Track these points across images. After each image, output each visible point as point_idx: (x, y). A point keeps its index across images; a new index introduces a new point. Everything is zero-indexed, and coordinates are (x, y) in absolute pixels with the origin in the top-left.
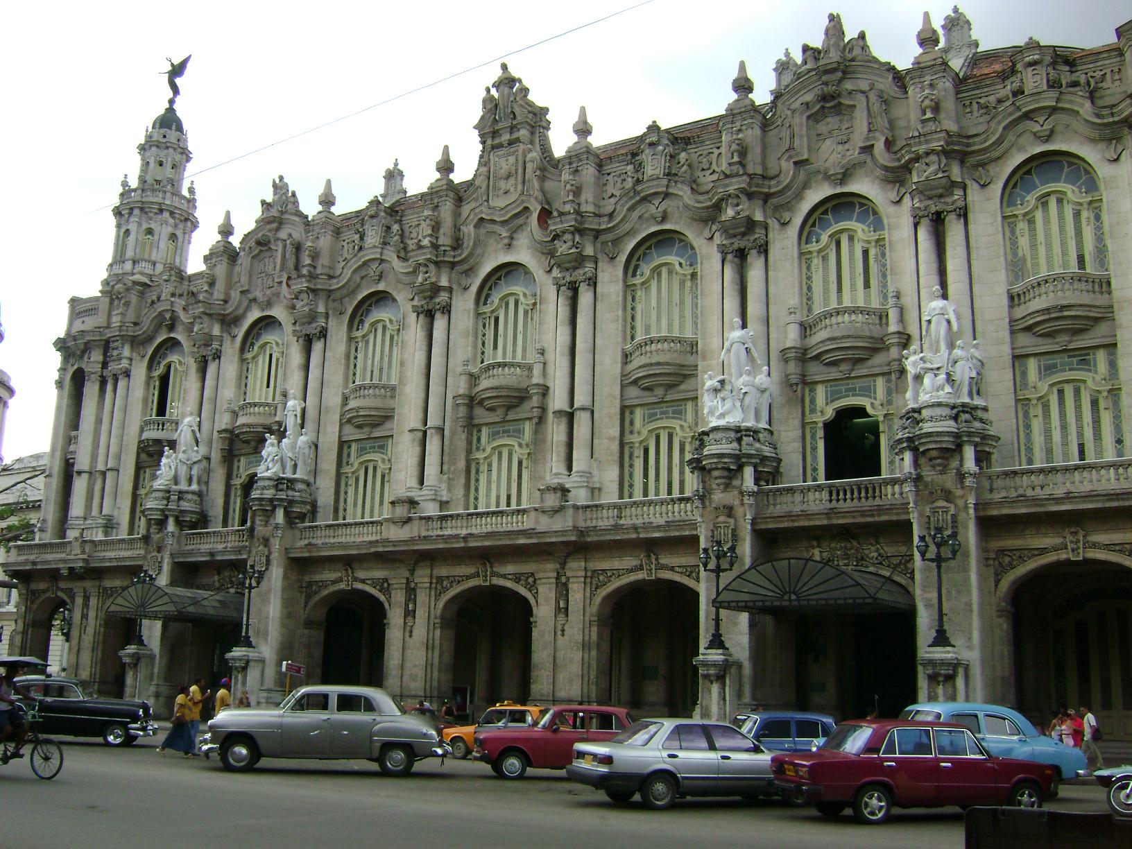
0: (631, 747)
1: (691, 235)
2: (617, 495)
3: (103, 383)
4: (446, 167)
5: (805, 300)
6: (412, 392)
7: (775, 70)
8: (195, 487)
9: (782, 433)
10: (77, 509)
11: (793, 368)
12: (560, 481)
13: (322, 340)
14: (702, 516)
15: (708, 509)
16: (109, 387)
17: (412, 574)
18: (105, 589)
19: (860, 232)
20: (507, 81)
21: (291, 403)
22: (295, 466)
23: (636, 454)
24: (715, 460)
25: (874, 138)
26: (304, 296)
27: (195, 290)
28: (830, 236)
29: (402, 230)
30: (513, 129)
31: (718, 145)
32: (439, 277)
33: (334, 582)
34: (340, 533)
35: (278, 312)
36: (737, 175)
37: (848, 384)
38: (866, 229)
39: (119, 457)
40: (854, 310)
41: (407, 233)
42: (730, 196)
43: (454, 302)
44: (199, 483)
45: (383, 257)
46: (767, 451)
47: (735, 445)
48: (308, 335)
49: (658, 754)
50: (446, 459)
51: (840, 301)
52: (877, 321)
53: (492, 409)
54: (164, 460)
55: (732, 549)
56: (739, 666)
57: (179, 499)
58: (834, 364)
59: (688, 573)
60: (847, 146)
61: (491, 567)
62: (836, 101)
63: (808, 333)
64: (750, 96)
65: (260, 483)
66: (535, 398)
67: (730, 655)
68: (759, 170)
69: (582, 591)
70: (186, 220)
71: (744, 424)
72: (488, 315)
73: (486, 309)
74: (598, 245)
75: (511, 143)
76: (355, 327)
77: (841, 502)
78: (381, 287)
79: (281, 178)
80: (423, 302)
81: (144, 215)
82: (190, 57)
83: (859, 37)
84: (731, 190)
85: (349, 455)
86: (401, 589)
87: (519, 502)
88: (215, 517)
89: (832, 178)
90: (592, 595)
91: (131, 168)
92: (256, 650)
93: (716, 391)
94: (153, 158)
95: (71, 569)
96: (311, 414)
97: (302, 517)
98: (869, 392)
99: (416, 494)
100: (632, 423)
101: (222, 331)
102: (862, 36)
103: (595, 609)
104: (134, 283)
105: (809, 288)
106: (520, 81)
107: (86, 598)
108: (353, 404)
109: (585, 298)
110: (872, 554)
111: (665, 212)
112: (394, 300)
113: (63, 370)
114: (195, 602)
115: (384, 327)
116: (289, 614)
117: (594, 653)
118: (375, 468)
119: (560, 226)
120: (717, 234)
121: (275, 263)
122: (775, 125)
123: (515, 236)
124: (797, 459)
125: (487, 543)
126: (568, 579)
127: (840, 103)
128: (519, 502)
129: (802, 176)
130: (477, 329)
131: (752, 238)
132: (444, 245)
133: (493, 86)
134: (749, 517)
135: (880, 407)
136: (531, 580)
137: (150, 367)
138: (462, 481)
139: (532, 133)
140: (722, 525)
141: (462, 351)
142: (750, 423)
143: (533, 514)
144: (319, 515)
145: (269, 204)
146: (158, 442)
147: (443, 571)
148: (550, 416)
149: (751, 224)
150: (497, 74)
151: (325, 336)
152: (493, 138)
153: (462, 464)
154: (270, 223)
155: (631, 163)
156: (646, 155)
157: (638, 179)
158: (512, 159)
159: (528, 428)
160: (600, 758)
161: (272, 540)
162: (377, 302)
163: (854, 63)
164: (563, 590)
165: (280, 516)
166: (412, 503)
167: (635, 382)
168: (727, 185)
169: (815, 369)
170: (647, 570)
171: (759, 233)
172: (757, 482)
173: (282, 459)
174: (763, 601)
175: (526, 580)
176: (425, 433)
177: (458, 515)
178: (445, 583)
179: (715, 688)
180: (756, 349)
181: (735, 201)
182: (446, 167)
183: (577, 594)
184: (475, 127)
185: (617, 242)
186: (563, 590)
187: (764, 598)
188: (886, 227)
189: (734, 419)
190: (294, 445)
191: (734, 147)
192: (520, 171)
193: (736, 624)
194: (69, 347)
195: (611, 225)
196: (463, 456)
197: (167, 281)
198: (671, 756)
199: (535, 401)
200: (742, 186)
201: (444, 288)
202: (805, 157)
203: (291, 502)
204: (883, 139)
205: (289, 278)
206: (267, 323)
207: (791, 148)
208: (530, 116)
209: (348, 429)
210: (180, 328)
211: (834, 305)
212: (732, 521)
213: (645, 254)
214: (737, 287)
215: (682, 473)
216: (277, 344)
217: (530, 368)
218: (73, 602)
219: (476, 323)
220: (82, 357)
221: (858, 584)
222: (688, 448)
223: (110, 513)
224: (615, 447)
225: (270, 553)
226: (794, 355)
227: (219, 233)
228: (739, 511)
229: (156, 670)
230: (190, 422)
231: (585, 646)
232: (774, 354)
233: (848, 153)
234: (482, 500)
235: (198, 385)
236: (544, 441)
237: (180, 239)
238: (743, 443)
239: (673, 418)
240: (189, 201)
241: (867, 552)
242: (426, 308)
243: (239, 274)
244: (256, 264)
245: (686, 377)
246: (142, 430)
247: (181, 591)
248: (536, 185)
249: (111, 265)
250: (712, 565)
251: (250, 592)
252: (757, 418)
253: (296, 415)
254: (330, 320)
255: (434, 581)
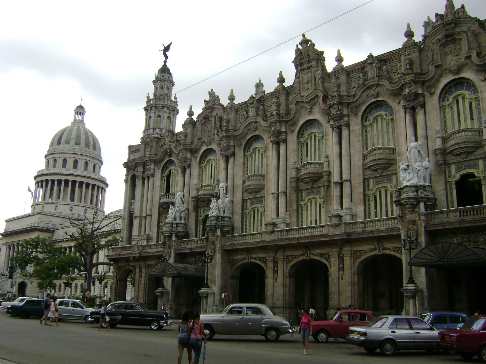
0: (375, 328)
1: (390, 102)
2: (363, 217)
3: (144, 180)
4: (281, 80)
5: (443, 127)
6: (272, 177)
7: (423, 26)
8: (183, 221)
9: (436, 187)
10: (135, 232)
11: (439, 157)
12: (338, 212)
13: (233, 157)
14: (402, 225)
15: (404, 222)
16: (146, 181)
17: (276, 255)
18: (148, 265)
19: (467, 95)
20: (305, 42)
21: (221, 184)
22: (224, 211)
23: (371, 199)
24: (407, 201)
25: (471, 52)
26: (224, 139)
27: (179, 139)
28: (453, 98)
29: (264, 108)
30: (309, 62)
31: (399, 61)
32: (281, 127)
33: (243, 259)
34: (244, 239)
35: (214, 146)
36: (409, 74)
37: (466, 163)
38: (470, 93)
39: (151, 210)
40: (466, 130)
41: (266, 110)
42: (406, 83)
43: (288, 138)
44: (184, 219)
45: (257, 121)
46: (430, 195)
47: (415, 193)
48: (227, 156)
49: (387, 331)
50: (288, 205)
51: (460, 127)
52: (478, 134)
53: (307, 183)
54: (170, 211)
55: (416, 239)
56: (422, 291)
57: (177, 226)
58: (459, 155)
59: (397, 251)
60: (459, 57)
61: (310, 251)
62: (452, 37)
63: (446, 142)
64: (413, 38)
65: (210, 219)
66: (325, 177)
67: (418, 287)
68: (419, 71)
69: (350, 260)
70: (174, 110)
71: (419, 184)
72: (303, 142)
73: (302, 140)
74: (349, 109)
75: (309, 68)
76: (246, 151)
77: (465, 217)
78: (257, 133)
79: (212, 90)
80: (275, 139)
81: (156, 110)
82: (171, 43)
83: (461, 8)
84: (407, 80)
85: (247, 205)
86: (271, 261)
87: (320, 222)
88: (192, 234)
89: (453, 72)
90: (354, 261)
91: (150, 90)
92: (211, 289)
93: (405, 170)
94: (159, 86)
95: (134, 257)
96: (230, 188)
97: (228, 232)
98: (476, 166)
99: (276, 221)
100: (368, 186)
101: (191, 156)
102: (463, 7)
103: (356, 268)
104: (154, 138)
105: (445, 122)
106: (310, 41)
107: (141, 269)
108: (247, 183)
109: (345, 133)
110: (481, 240)
111: (378, 93)
112: (263, 139)
113: (127, 175)
114: (185, 269)
115: (259, 150)
116: (224, 273)
117: (356, 287)
118: (258, 210)
119: (332, 102)
120: (402, 101)
121: (211, 126)
122: (425, 50)
123: (313, 108)
124: (444, 198)
125: (307, 241)
126: (343, 255)
127: (454, 38)
128: (320, 222)
129: (439, 72)
130: (298, 149)
131: (418, 101)
132: (282, 114)
133: (299, 44)
134: (423, 225)
135: (481, 173)
136: (327, 256)
137: (162, 172)
138: (296, 214)
139: (318, 63)
140: (411, 229)
141: (293, 158)
142: (422, 183)
143: (327, 227)
144: (235, 231)
145: (207, 101)
146: (167, 203)
147: (289, 253)
148: (332, 184)
149: (417, 95)
150: (301, 38)
151: (234, 156)
152: (301, 66)
153: (295, 207)
154: (208, 109)
155: (362, 72)
156: (368, 69)
157: (365, 79)
158: (309, 75)
159: (323, 190)
160: (361, 334)
161: (216, 243)
162: (255, 139)
163: (460, 19)
164: (341, 260)
165: (219, 233)
166: (274, 225)
167: (369, 168)
168: (405, 79)
169: (450, 158)
170: (378, 250)
171: (421, 99)
172: (426, 209)
173: (218, 208)
174: (432, 262)
175: (325, 256)
176: (278, 194)
177: (294, 229)
178: (290, 258)
179: (411, 301)
180: (422, 150)
181: (409, 86)
182: (281, 80)
183: (348, 261)
184: (293, 62)
185: (358, 107)
186: (341, 260)
187: (432, 261)
188: (479, 92)
189: (414, 181)
190: (223, 202)
191: (407, 62)
192: (313, 80)
193: (419, 273)
194: (129, 166)
195: (354, 100)
196: (295, 204)
197: (167, 136)
198: (392, 332)
199: (325, 178)
200: (412, 78)
201: (283, 132)
202: (440, 63)
203: (223, 226)
204: (475, 52)
205: (218, 132)
206: (210, 151)
207: (433, 60)
208: (316, 55)
209: (246, 194)
210: (174, 155)
211: (457, 128)
212: (415, 227)
213: (370, 112)
214: (412, 123)
215: (392, 207)
216: (214, 160)
217: (322, 164)
218: (135, 271)
219: (298, 146)
220: (134, 170)
221: (475, 253)
222: (394, 195)
223: (149, 234)
224: (361, 196)
225: (215, 248)
226: (439, 152)
227: (188, 115)
228: (419, 222)
229: (170, 298)
230: (179, 194)
231: (352, 284)
232: (431, 152)
233: (460, 60)
234: (304, 222)
235: (182, 179)
236: (330, 195)
237: (172, 119)
238: (419, 192)
239: (387, 183)
240: (174, 102)
241: (478, 239)
242: (276, 141)
243: (197, 132)
244: (203, 126)
245: (392, 164)
246: (160, 199)
247: (179, 265)
248: (321, 85)
249: (144, 131)
250: (407, 247)
251: (207, 265)
252: (425, 181)
253: (223, 190)
254: (236, 148)
255: (285, 257)
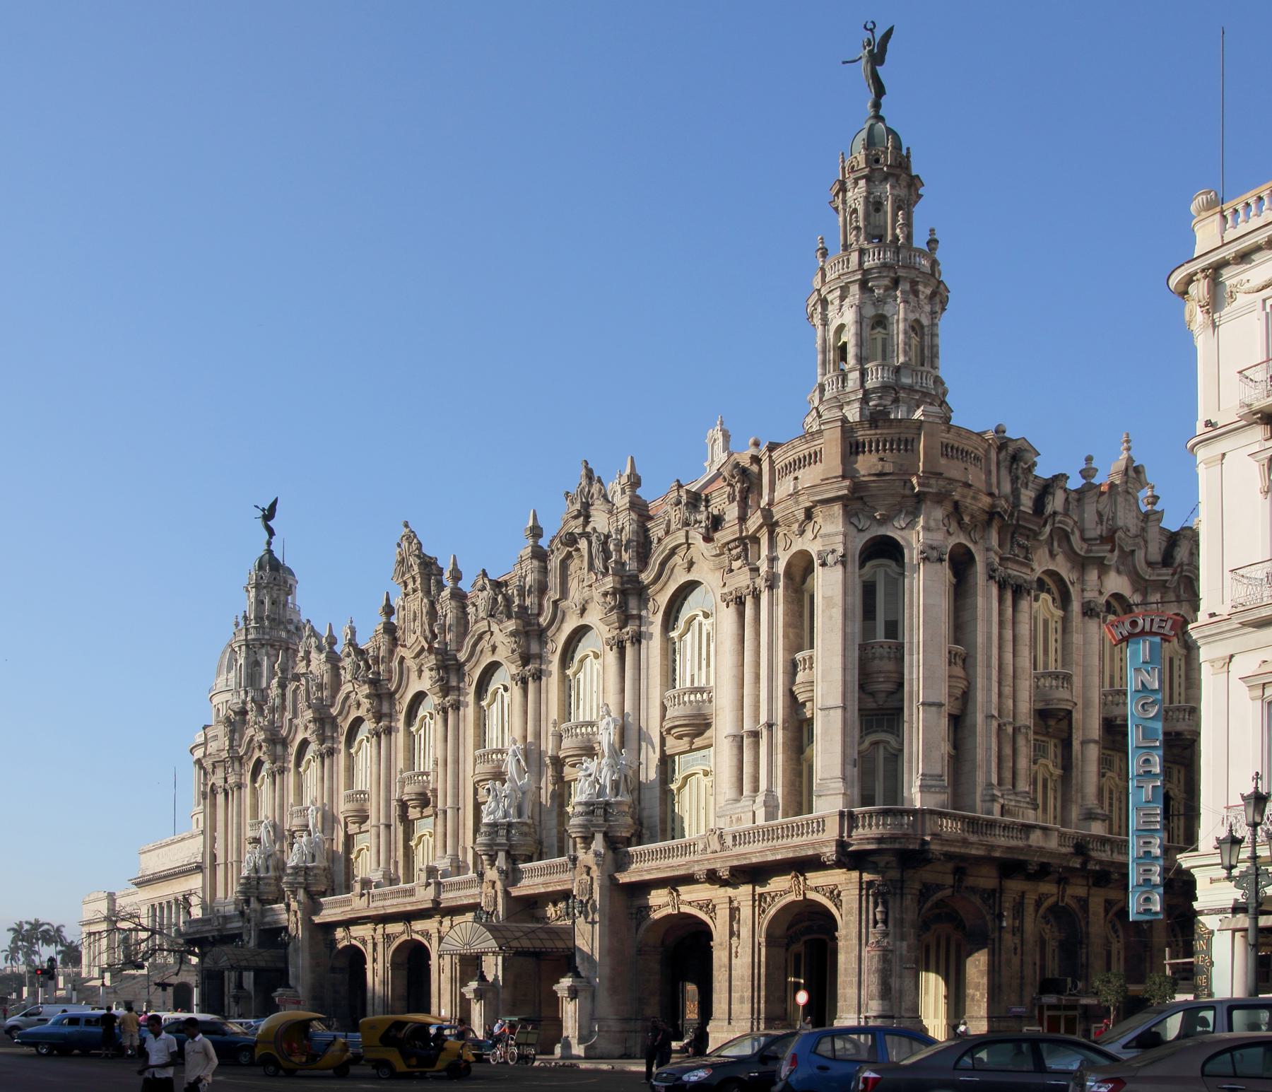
8: (271, 873)
50: (393, 847)
82: (276, 499)
91: (246, 603)
95: (213, 937)
124: (555, 841)
